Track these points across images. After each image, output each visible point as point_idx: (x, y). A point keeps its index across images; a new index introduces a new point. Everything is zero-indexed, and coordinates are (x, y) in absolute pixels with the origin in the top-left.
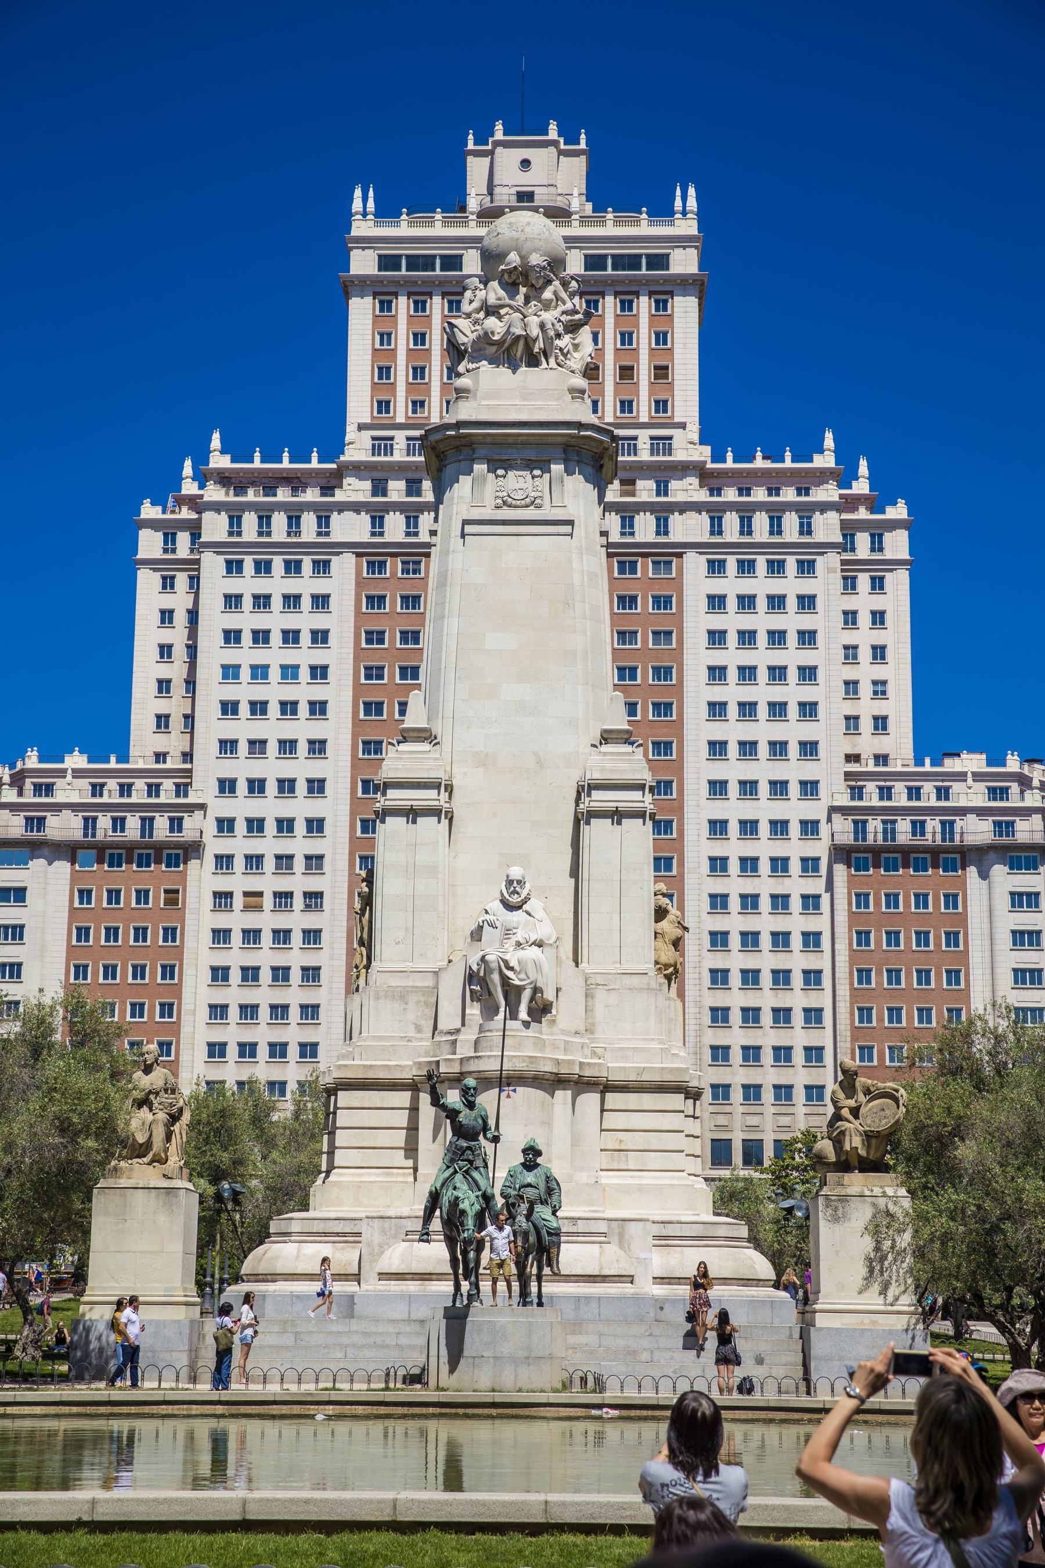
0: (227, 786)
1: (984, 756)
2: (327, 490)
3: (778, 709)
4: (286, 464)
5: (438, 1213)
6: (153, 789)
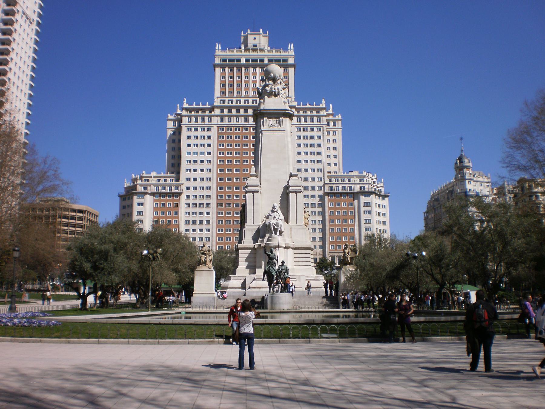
0: (189, 179)
1: (358, 172)
2: (210, 112)
3: (313, 162)
4: (201, 106)
5: (266, 275)
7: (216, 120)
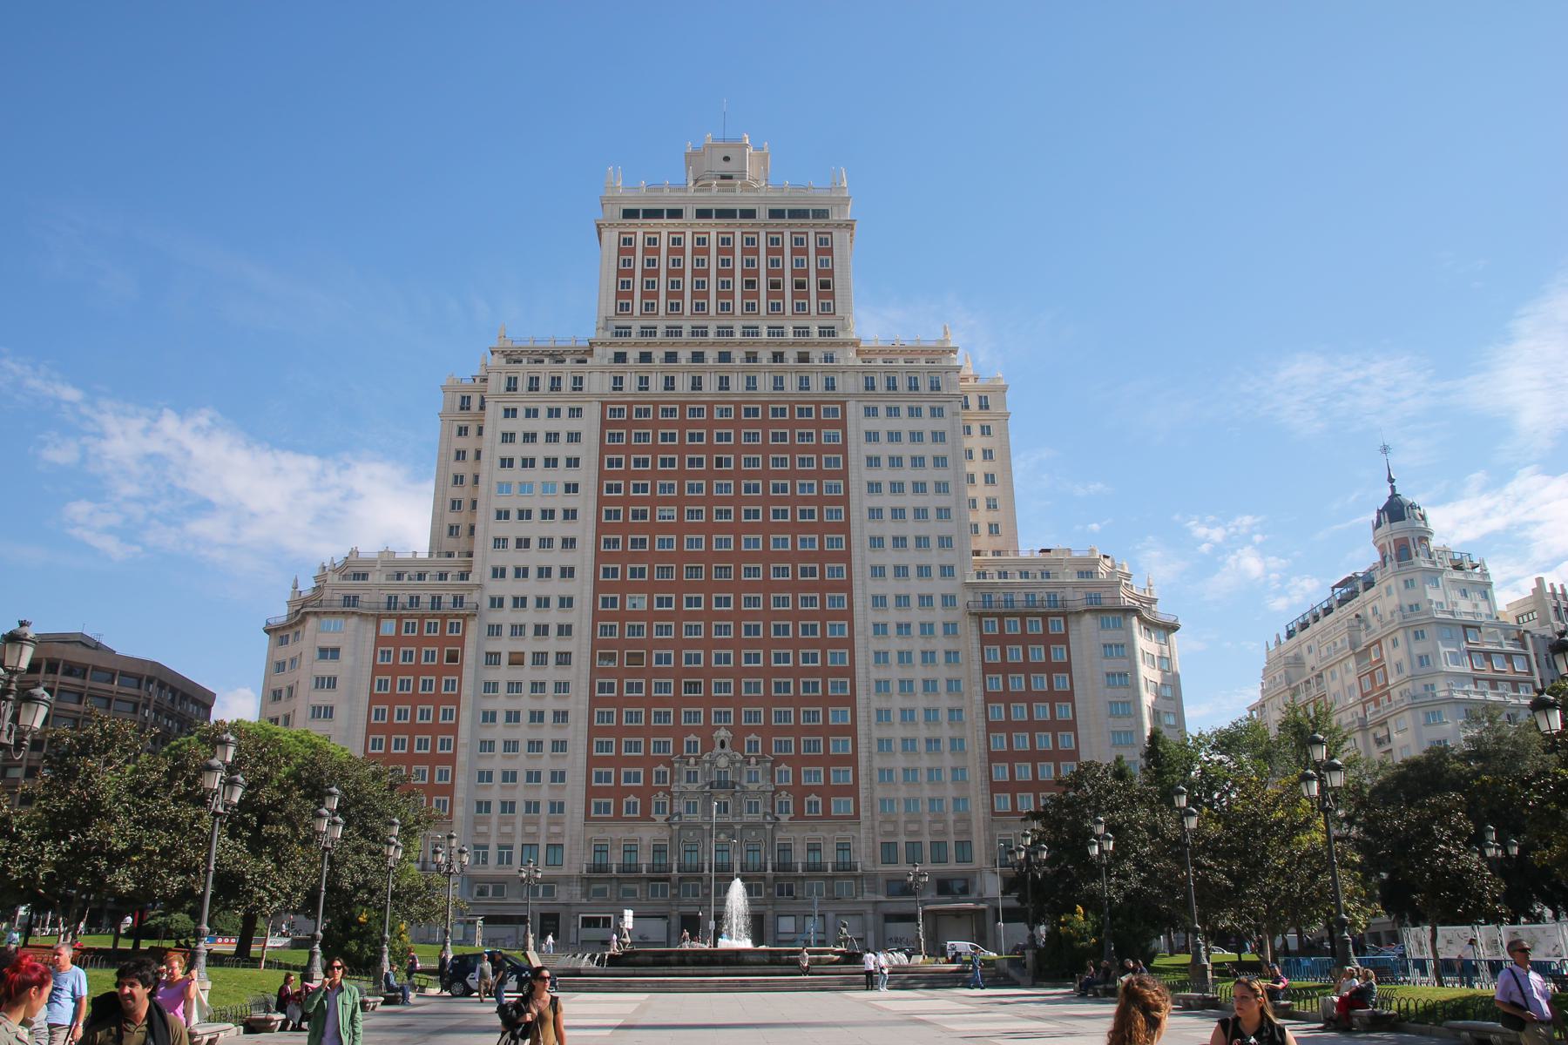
6: (443, 576)
7: (597, 383)
